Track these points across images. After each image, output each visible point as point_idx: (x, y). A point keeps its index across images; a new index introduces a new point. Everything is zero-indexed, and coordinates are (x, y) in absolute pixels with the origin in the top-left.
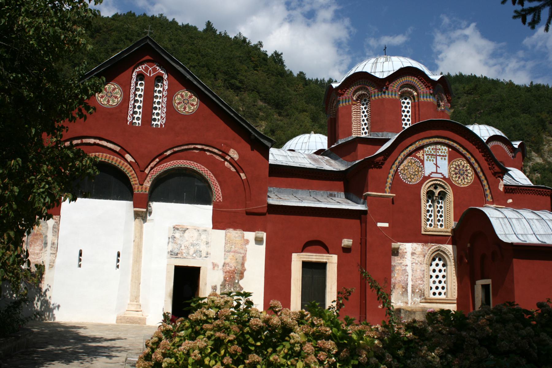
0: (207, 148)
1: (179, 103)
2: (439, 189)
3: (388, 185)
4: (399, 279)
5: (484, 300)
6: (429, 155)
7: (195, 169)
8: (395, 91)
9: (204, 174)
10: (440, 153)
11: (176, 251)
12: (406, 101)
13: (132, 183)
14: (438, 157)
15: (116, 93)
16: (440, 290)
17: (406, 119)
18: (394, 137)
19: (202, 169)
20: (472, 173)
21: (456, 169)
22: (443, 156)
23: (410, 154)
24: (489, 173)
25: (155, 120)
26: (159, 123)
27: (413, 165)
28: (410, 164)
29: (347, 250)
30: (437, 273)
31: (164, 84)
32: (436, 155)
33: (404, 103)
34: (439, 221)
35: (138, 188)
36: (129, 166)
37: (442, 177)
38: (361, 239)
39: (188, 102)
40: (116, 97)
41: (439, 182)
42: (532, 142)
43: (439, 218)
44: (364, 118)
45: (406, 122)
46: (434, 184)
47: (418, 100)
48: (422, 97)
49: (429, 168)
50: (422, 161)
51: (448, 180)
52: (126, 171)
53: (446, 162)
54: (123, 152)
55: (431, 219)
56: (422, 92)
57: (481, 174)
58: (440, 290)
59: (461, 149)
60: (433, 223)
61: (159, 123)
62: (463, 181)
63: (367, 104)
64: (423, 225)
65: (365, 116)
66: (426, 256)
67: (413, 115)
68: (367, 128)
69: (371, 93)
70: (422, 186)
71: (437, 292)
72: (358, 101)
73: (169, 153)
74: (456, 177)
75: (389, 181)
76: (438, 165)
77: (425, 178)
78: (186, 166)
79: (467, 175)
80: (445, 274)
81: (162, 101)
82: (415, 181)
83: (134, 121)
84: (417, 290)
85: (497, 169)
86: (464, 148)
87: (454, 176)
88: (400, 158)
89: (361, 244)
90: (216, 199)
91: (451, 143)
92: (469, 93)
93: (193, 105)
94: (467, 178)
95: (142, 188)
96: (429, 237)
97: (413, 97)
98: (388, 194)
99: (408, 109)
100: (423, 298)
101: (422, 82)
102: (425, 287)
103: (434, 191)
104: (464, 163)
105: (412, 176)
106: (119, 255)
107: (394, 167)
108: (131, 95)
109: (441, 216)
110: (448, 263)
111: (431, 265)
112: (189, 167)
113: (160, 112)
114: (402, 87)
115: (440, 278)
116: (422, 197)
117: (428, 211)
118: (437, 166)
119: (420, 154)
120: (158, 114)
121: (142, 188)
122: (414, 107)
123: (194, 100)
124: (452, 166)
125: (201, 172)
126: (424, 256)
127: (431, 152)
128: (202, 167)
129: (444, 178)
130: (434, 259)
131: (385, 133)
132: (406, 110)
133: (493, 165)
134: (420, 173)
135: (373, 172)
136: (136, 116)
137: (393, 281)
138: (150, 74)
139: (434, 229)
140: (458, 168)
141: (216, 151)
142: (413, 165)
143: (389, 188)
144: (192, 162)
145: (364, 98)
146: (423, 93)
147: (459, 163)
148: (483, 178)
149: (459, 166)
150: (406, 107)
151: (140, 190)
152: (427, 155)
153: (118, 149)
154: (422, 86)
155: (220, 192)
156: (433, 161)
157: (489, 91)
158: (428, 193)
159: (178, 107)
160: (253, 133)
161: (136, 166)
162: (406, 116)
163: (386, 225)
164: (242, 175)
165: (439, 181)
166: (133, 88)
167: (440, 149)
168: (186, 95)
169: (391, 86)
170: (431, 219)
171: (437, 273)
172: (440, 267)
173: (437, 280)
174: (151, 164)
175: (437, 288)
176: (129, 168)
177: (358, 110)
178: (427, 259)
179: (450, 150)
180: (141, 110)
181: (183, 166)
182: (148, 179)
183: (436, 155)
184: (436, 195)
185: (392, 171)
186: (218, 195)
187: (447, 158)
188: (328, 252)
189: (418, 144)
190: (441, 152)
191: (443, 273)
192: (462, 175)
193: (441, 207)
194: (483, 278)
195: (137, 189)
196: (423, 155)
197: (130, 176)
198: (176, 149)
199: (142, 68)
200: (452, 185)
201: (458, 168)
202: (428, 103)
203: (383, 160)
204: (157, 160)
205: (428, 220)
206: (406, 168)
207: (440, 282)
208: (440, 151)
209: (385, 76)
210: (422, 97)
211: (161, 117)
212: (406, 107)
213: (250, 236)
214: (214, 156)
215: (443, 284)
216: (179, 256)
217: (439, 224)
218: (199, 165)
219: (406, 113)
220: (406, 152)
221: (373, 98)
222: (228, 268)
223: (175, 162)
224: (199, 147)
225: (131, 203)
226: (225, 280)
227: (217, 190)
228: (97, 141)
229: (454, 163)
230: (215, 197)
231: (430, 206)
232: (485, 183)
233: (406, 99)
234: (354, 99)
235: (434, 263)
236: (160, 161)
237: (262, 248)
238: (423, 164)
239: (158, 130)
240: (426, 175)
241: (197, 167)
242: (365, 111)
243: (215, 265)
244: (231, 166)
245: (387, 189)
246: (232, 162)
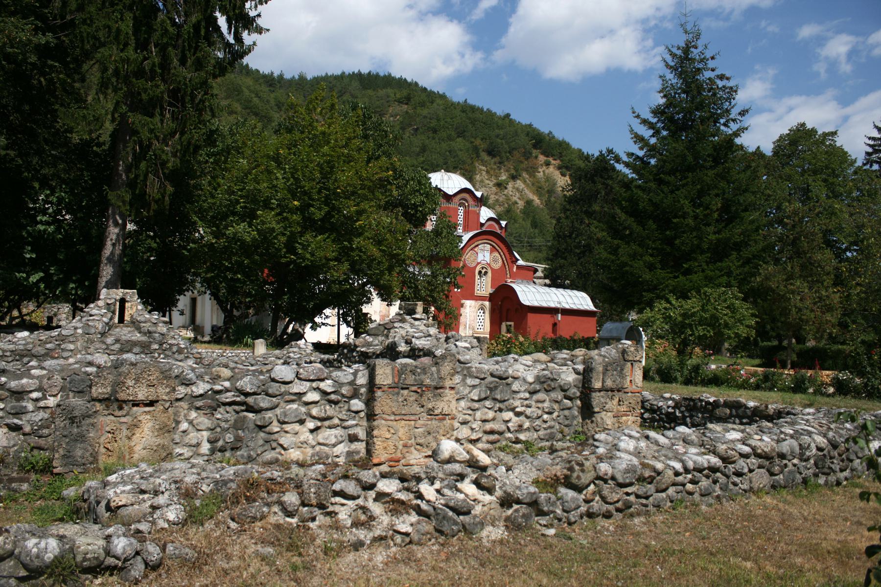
24: (509, 261)
42: (466, 170)
49: (480, 258)
51: (489, 264)
77: (478, 263)
82: (473, 265)
92: (400, 102)
104: (497, 255)
119: (476, 249)
122: (465, 213)
157: (423, 105)
243: (375, 312)
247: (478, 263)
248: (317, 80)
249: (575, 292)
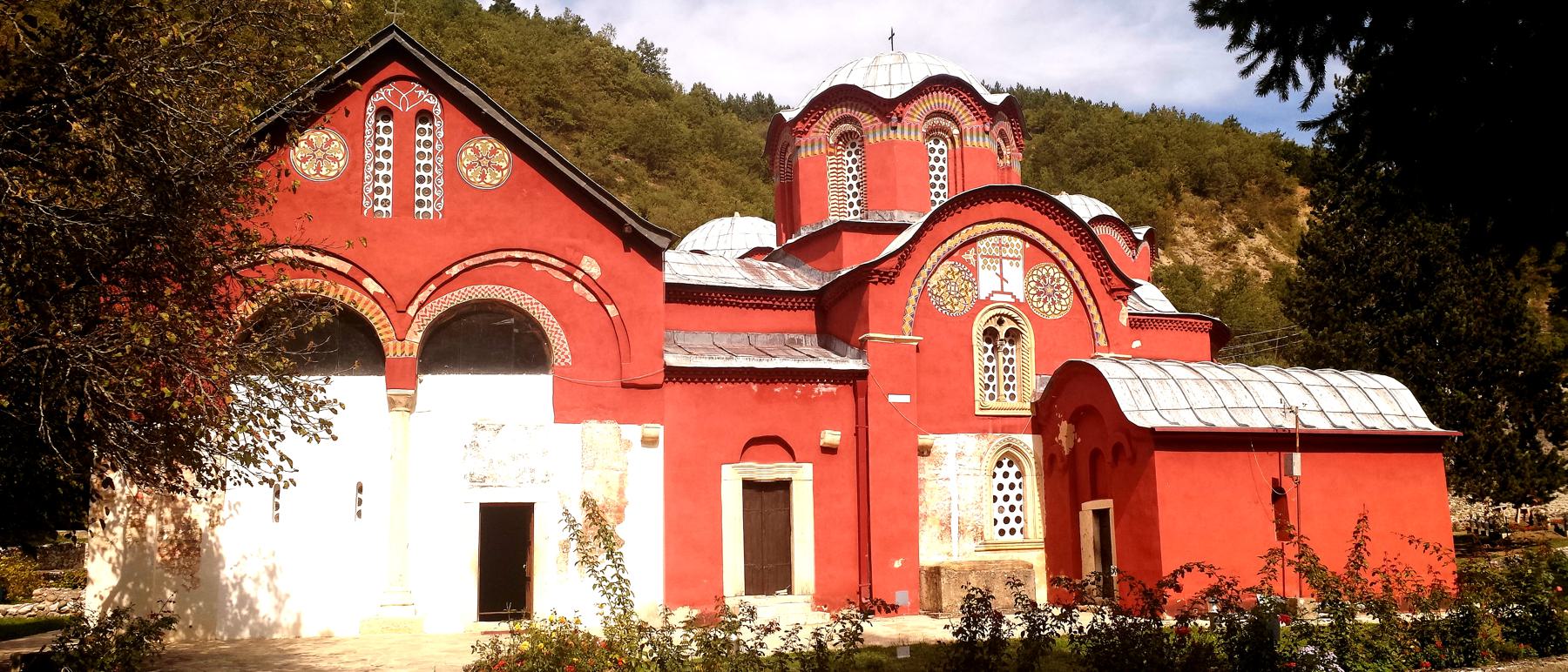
0: (534, 257)
1: (470, 167)
2: (1008, 325)
3: (908, 318)
5: (1098, 539)
6: (988, 257)
7: (512, 300)
8: (916, 127)
9: (531, 311)
10: (1008, 253)
11: (478, 474)
12: (937, 148)
13: (381, 338)
14: (1004, 261)
15: (336, 150)
16: (1013, 524)
17: (938, 183)
18: (917, 222)
19: (527, 301)
20: (1068, 292)
21: (1038, 283)
22: (1014, 259)
23: (949, 256)
24: (1100, 290)
25: (421, 203)
26: (431, 210)
27: (956, 277)
28: (950, 276)
29: (829, 450)
30: (1006, 490)
31: (435, 128)
32: (1002, 258)
33: (933, 150)
34: (1007, 387)
35: (395, 348)
36: (372, 302)
37: (1013, 300)
38: (857, 428)
39: (489, 163)
40: (335, 160)
41: (1005, 311)
43: (1007, 381)
44: (851, 181)
45: (937, 189)
46: (997, 315)
47: (962, 146)
48: (968, 138)
50: (974, 270)
52: (367, 314)
53: (1020, 270)
54: (357, 275)
55: (991, 384)
56: (968, 129)
57: (1086, 294)
58: (1013, 524)
59: (1049, 245)
60: (995, 393)
61: (431, 210)
62: (1053, 309)
63: (857, 153)
64: (977, 397)
65: (855, 177)
66: (986, 458)
67: (952, 175)
68: (859, 203)
69: (867, 129)
70: (973, 319)
71: (1007, 528)
72: (839, 147)
73: (455, 270)
74: (1039, 300)
75: (910, 309)
76: (1004, 276)
77: (980, 304)
78: (493, 296)
79: (1060, 297)
80: (1020, 491)
81: (434, 162)
83: (376, 208)
84: (970, 528)
85: (1116, 282)
86: (1054, 243)
87: (1036, 298)
88: (930, 264)
89: (856, 435)
90: (559, 361)
91: (1029, 232)
93: (499, 168)
94: (1059, 302)
95: (403, 347)
97: (952, 138)
99: (941, 163)
100: (980, 542)
101: (969, 107)
102: (984, 521)
103: (998, 328)
104: (1054, 271)
105: (955, 301)
106: (360, 490)
107: (919, 283)
108: (367, 153)
109: (1012, 378)
110: (1028, 471)
111: (994, 475)
112: (499, 297)
113: (430, 186)
114: (928, 118)
115: (1012, 501)
116: (975, 341)
117: (987, 369)
118: (1003, 279)
119: (969, 256)
120: (427, 192)
121: (403, 347)
122: (953, 157)
123: (501, 159)
124: (1031, 279)
125: (524, 307)
126: (982, 459)
127: (990, 250)
128: (527, 296)
129: (1017, 303)
130: (999, 464)
131: (896, 213)
132: (937, 165)
133: (1107, 274)
134: (970, 294)
136: (381, 197)
137: (922, 510)
138: (404, 108)
139: (999, 405)
140: (1042, 281)
141: (553, 261)
142: (956, 277)
143: (911, 324)
144: (504, 288)
145: (851, 141)
146: (971, 130)
147: (1045, 272)
148: (1090, 301)
149: (1044, 277)
150: (937, 159)
151: (399, 353)
152: (982, 256)
153: (346, 268)
154: (969, 115)
155: (566, 345)
156: (995, 268)
158: (985, 332)
159: (470, 174)
160: (629, 221)
161: (386, 302)
162: (937, 178)
163: (906, 399)
164: (610, 308)
165: (1007, 308)
166: (370, 139)
167: (1008, 246)
168: (485, 147)
169: (908, 115)
170: (991, 384)
171: (1006, 490)
172: (1012, 478)
173: (1007, 505)
174: (420, 296)
175: (1007, 520)
176: (372, 308)
177: (840, 166)
178: (990, 462)
179: (1028, 245)
180: (390, 184)
181: (486, 296)
182: (414, 326)
183: (1002, 258)
184: (1002, 336)
185: (915, 291)
186: (563, 353)
187: (1021, 263)
189: (965, 235)
190: (1011, 251)
191: (1017, 491)
192: (1050, 296)
193: (1011, 360)
194: (1095, 497)
195: (393, 349)
196: (975, 257)
197: (376, 324)
198: (469, 263)
199: (386, 93)
200: (1032, 317)
201: (1042, 281)
202: (982, 152)
203: (897, 268)
204: (432, 287)
205: (987, 387)
206: (943, 283)
207: (1012, 508)
208: (1007, 250)
209: (894, 96)
210: (968, 138)
211: (435, 197)
212: (937, 159)
214: (551, 271)
215: (1017, 513)
216: (488, 482)
217: (1008, 393)
218: (519, 292)
219: (937, 172)
220: (941, 252)
221: (871, 140)
223: (469, 288)
224: (518, 255)
225: (380, 381)
227: (561, 343)
228: (300, 254)
229: (1035, 272)
230: (557, 357)
231: (990, 359)
232: (1093, 311)
233: (937, 142)
234: (831, 142)
235: (1000, 472)
236: (438, 288)
237: (656, 458)
238: (976, 275)
239: (430, 226)
240: (982, 297)
241: (517, 298)
242: (854, 167)
244: (587, 291)
245: (907, 327)
247: (980, 304)
249: (1358, 376)
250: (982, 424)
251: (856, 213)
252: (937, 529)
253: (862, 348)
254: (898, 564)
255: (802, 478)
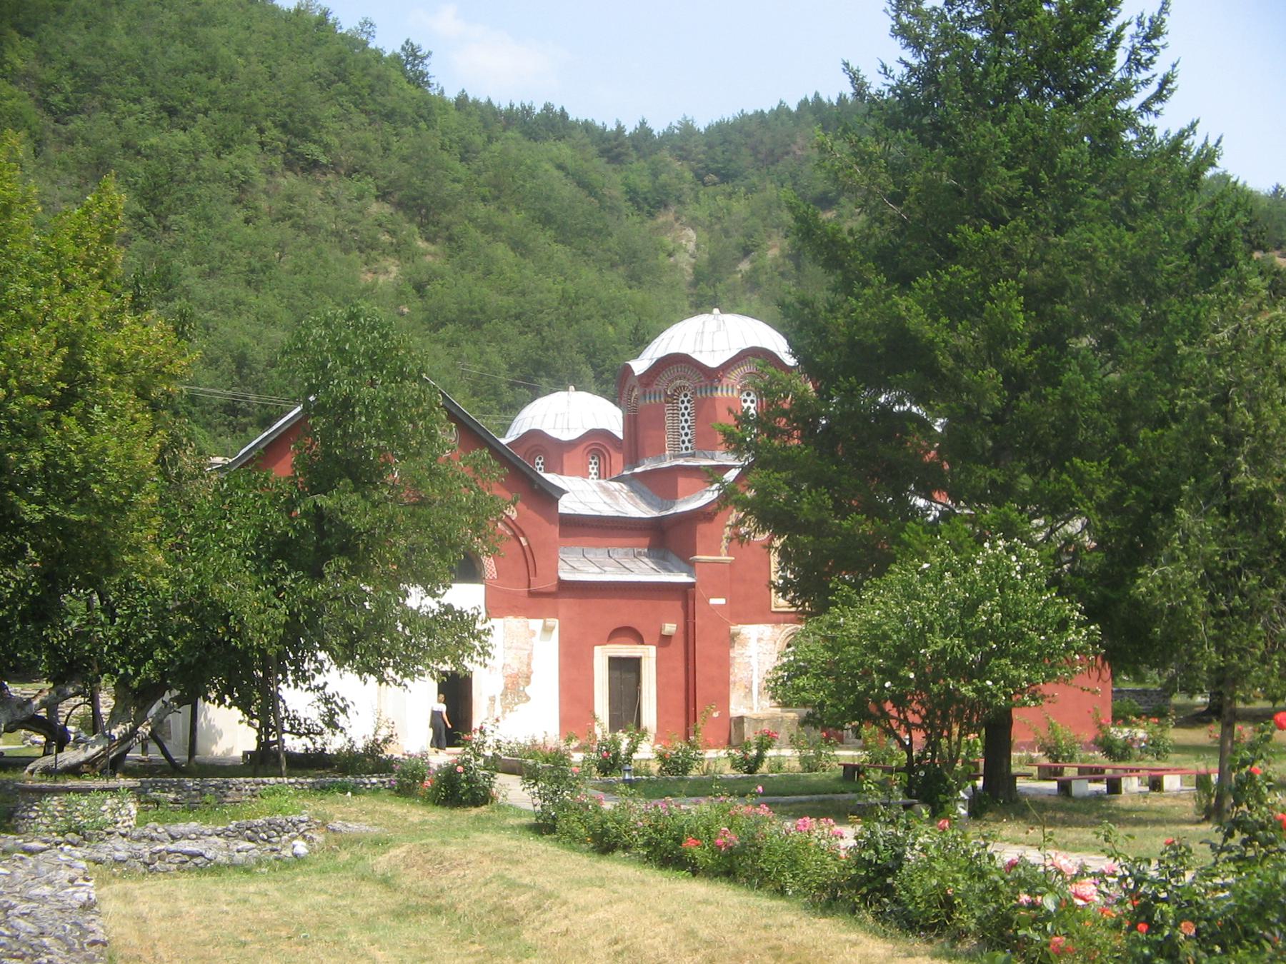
4: (740, 675)
12: (749, 399)
96: (782, 617)
98: (723, 558)
135: (702, 528)
137: (732, 678)
163: (722, 601)
164: (522, 539)
188: (642, 643)
213: (537, 624)
222: (509, 671)
226: (506, 688)
233: (748, 395)
245: (723, 550)
246: (509, 523)
248: (722, 132)
250: (775, 617)
251: (687, 448)
252: (742, 692)
253: (690, 566)
254: (716, 715)
255: (648, 654)
